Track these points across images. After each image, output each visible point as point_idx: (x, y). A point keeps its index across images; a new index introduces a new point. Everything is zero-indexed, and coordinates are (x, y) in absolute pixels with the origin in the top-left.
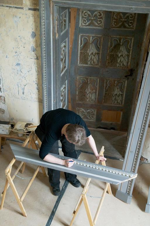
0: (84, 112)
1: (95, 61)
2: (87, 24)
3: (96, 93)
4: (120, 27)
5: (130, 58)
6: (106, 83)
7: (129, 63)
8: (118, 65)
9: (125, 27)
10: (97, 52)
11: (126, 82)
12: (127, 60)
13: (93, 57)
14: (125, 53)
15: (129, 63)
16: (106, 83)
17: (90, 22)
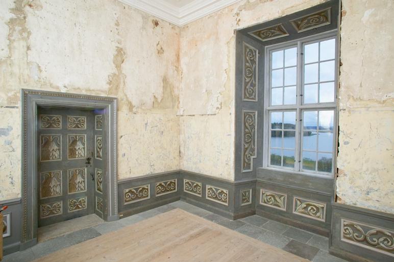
0: (49, 208)
1: (56, 155)
2: (47, 126)
3: (60, 185)
4: (75, 127)
5: (86, 150)
6: (69, 173)
7: (86, 154)
8: (77, 156)
9: (79, 127)
10: (58, 148)
11: (86, 169)
12: (83, 151)
13: (54, 153)
14: (81, 146)
15: (86, 154)
16: (69, 173)
17: (49, 124)
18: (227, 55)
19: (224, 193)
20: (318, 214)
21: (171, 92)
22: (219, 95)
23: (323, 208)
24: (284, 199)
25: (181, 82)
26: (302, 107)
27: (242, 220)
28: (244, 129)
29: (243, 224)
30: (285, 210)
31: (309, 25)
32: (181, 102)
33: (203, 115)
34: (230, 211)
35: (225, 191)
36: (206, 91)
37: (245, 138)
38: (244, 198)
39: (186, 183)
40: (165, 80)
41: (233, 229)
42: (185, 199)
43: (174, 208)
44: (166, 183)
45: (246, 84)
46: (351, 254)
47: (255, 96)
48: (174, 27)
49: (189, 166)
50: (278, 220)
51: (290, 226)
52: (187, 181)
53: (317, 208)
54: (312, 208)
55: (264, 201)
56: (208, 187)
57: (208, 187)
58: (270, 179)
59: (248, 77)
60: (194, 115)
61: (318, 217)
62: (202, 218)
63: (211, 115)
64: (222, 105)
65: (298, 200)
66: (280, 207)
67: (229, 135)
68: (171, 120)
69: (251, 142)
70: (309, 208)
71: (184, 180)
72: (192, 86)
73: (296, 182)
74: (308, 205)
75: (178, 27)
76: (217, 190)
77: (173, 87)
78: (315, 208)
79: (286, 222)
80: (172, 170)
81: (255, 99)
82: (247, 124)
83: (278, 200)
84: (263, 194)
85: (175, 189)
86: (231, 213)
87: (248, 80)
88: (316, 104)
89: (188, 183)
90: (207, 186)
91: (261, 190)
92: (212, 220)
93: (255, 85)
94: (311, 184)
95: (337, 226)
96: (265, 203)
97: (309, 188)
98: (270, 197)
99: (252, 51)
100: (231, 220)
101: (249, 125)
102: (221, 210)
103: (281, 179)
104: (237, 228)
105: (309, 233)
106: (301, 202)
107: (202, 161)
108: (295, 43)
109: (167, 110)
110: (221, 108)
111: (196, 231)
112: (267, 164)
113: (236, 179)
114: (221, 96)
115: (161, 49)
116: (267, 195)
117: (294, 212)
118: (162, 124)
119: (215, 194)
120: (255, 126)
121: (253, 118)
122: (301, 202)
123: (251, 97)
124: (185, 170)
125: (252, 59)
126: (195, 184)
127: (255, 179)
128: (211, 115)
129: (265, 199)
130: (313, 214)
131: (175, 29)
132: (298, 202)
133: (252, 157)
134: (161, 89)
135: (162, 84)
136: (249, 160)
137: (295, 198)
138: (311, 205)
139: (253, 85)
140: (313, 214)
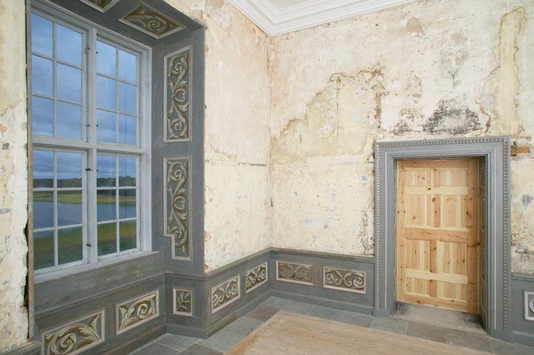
23: (154, 298)
31: (144, 23)
46: (219, 322)
53: (148, 303)
58: (67, 298)
65: (122, 307)
66: (90, 342)
70: (139, 309)
73: (117, 278)
78: (145, 305)
83: (86, 330)
95: (209, 299)
97: (138, 278)
103: (92, 286)
106: (126, 307)
116: (59, 338)
122: (126, 307)
130: (144, 315)
132: (123, 311)
140: (144, 315)
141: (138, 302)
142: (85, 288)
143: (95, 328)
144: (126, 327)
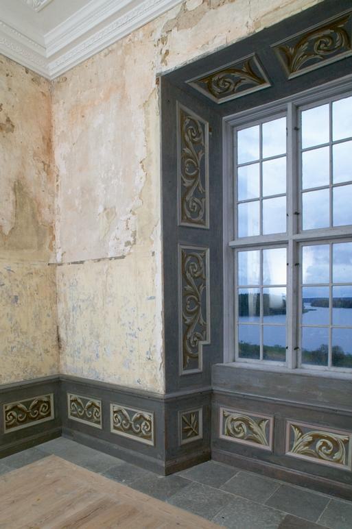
18: (145, 131)
19: (146, 419)
20: (337, 456)
21: (34, 216)
22: (130, 215)
24: (268, 425)
25: (57, 195)
26: (298, 237)
27: (182, 474)
28: (184, 285)
29: (184, 484)
30: (269, 448)
32: (58, 237)
33: (99, 260)
34: (159, 456)
35: (146, 415)
36: (105, 209)
37: (185, 304)
38: (186, 428)
39: (72, 401)
40: (19, 188)
41: (163, 499)
42: (70, 435)
43: (45, 455)
44: (27, 404)
45: (185, 191)
47: (204, 218)
48: (36, 79)
49: (75, 365)
50: (257, 470)
51: (282, 483)
52: (74, 396)
53: (336, 443)
54: (325, 444)
55: (228, 431)
56: (114, 407)
57: (114, 407)
58: (238, 388)
59: (187, 177)
60: (82, 262)
61: (338, 461)
62: (99, 475)
63: (116, 258)
64: (137, 237)
65: (296, 427)
66: (258, 442)
67: (151, 298)
68: (37, 273)
69: (197, 311)
70: (319, 444)
71: (69, 396)
72: (77, 202)
73: (290, 391)
74: (316, 438)
75: (47, 80)
76: (131, 413)
77: (39, 205)
78: (330, 443)
79: (273, 474)
80: (43, 375)
81: (203, 223)
82: (188, 275)
83: (255, 428)
84: (225, 417)
85: (49, 415)
86: (161, 461)
87: (188, 183)
88: (326, 230)
89: (75, 401)
90: (111, 406)
91: (221, 410)
92: (119, 479)
93: (203, 196)
94: (321, 394)
96: (230, 435)
98: (239, 423)
99: (196, 123)
100: (161, 477)
101: (194, 278)
102: (141, 455)
104: (171, 494)
105: (321, 494)
106: (302, 431)
107: (100, 354)
108: (279, 108)
109: (25, 251)
110: (135, 243)
111: (81, 508)
112: (232, 359)
113: (168, 390)
114: (133, 218)
115: (8, 120)
116: (233, 420)
117: (288, 454)
118: (16, 280)
119: (127, 421)
120: (205, 279)
121: (201, 264)
122: (302, 431)
123: (196, 219)
124: (70, 374)
125: (196, 139)
126: (89, 403)
127: (209, 388)
128: (116, 258)
129: (230, 427)
130: (327, 455)
131: (39, 84)
132: (296, 432)
133: (201, 343)
134: (11, 208)
135: (12, 197)
136: (196, 349)
137: (289, 423)
138: (323, 438)
139: (199, 195)
140: (327, 455)
141: (321, 433)
142: (255, 385)
143: (264, 430)
144: (298, 452)
